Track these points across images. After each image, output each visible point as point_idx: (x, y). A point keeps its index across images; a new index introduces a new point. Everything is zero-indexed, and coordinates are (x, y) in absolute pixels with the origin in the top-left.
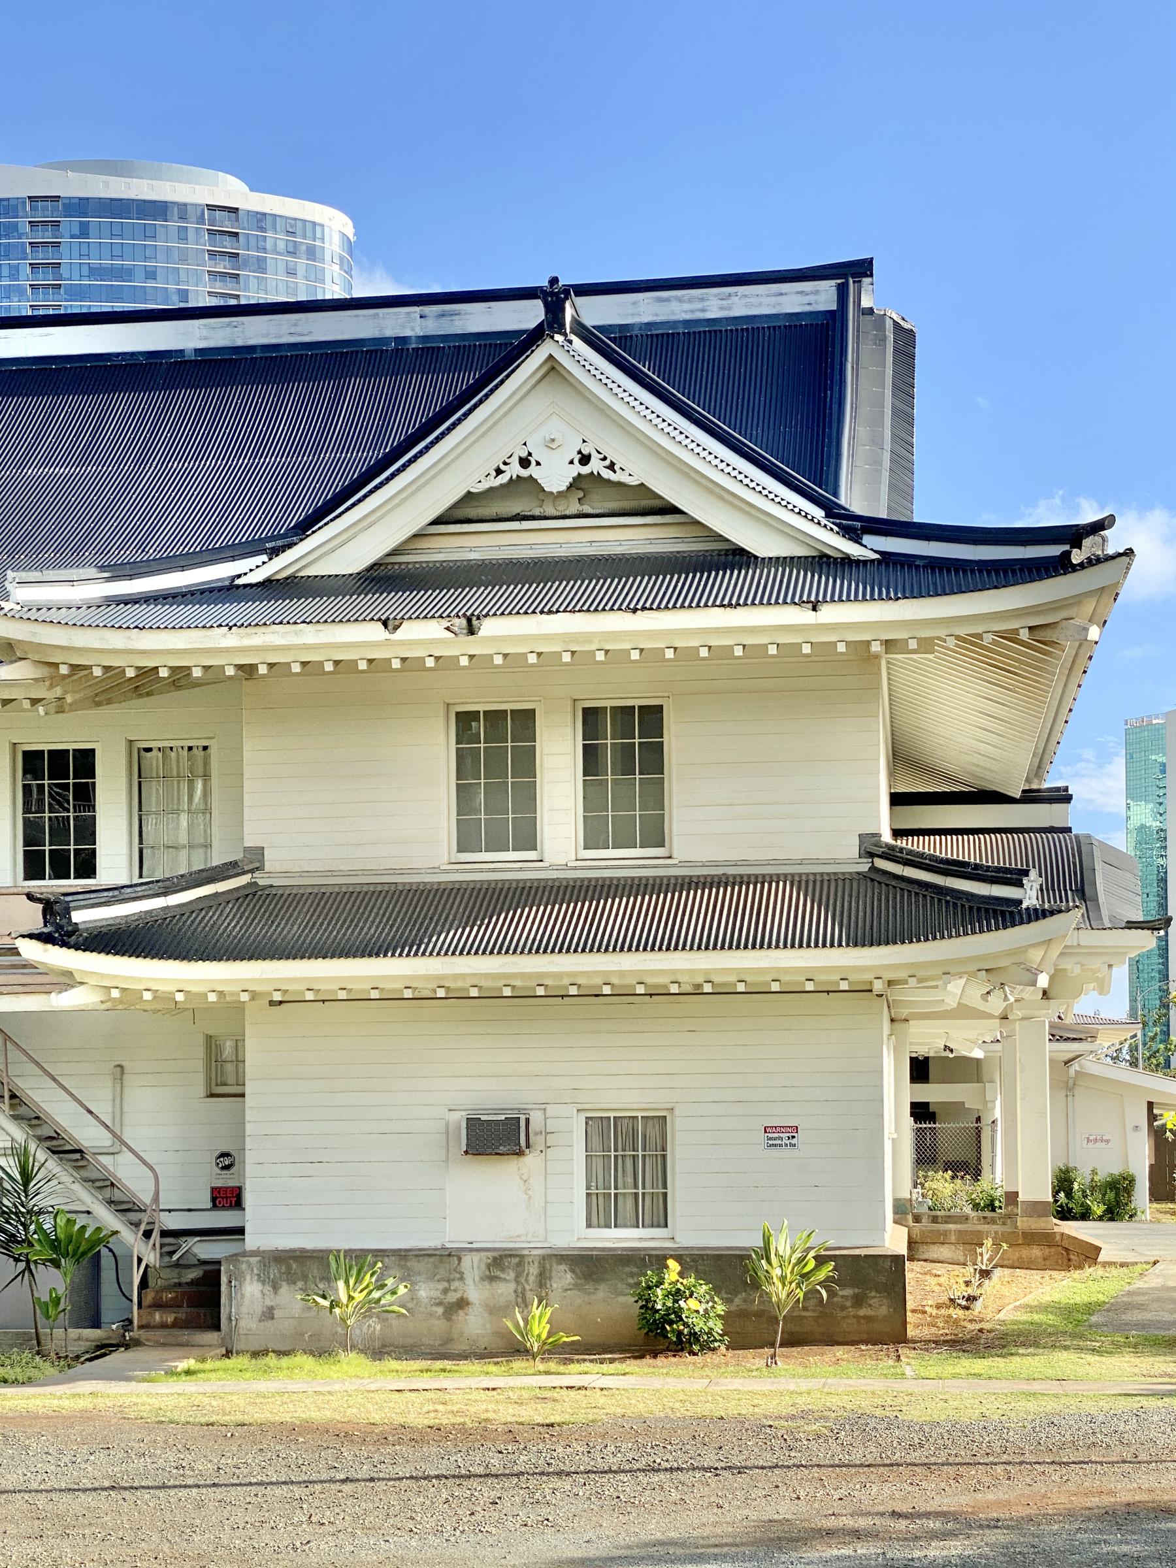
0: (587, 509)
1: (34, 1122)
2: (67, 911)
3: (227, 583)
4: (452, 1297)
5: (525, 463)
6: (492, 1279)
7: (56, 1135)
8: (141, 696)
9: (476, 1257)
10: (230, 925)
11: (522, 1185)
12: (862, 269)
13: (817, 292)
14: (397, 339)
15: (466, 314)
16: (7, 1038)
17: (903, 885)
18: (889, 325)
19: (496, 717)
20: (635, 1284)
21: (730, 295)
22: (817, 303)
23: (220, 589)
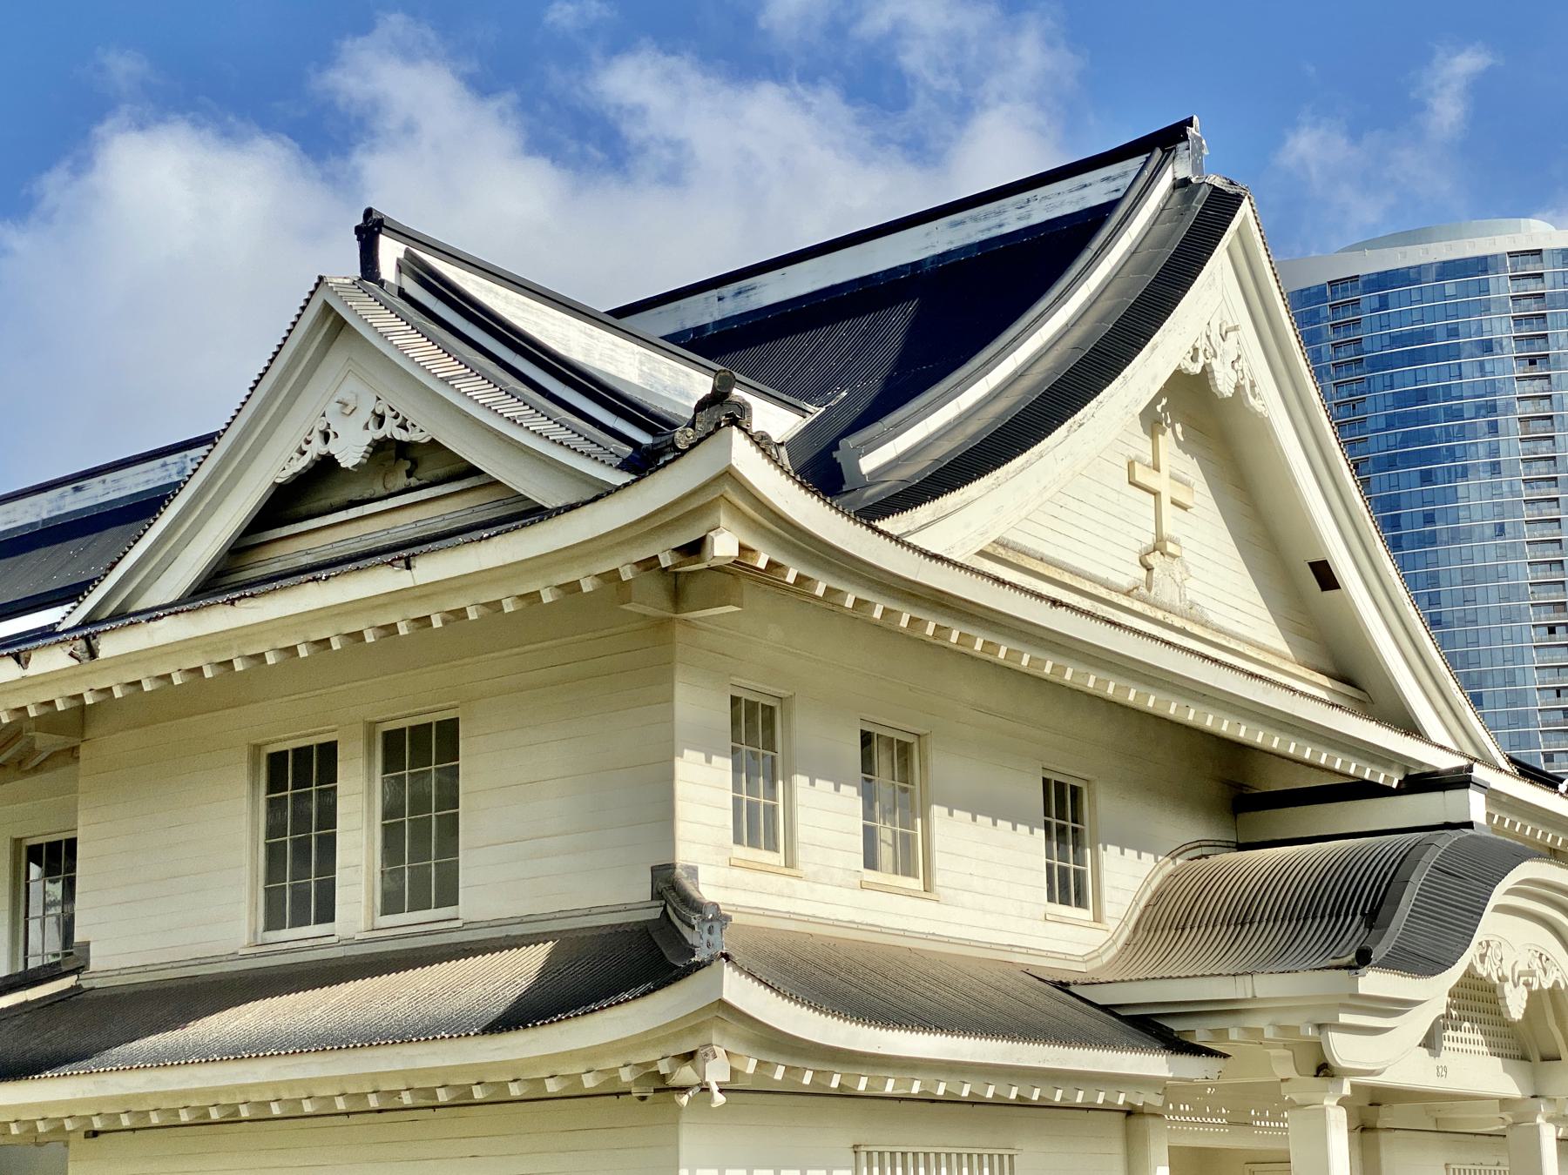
21: (1028, 201)
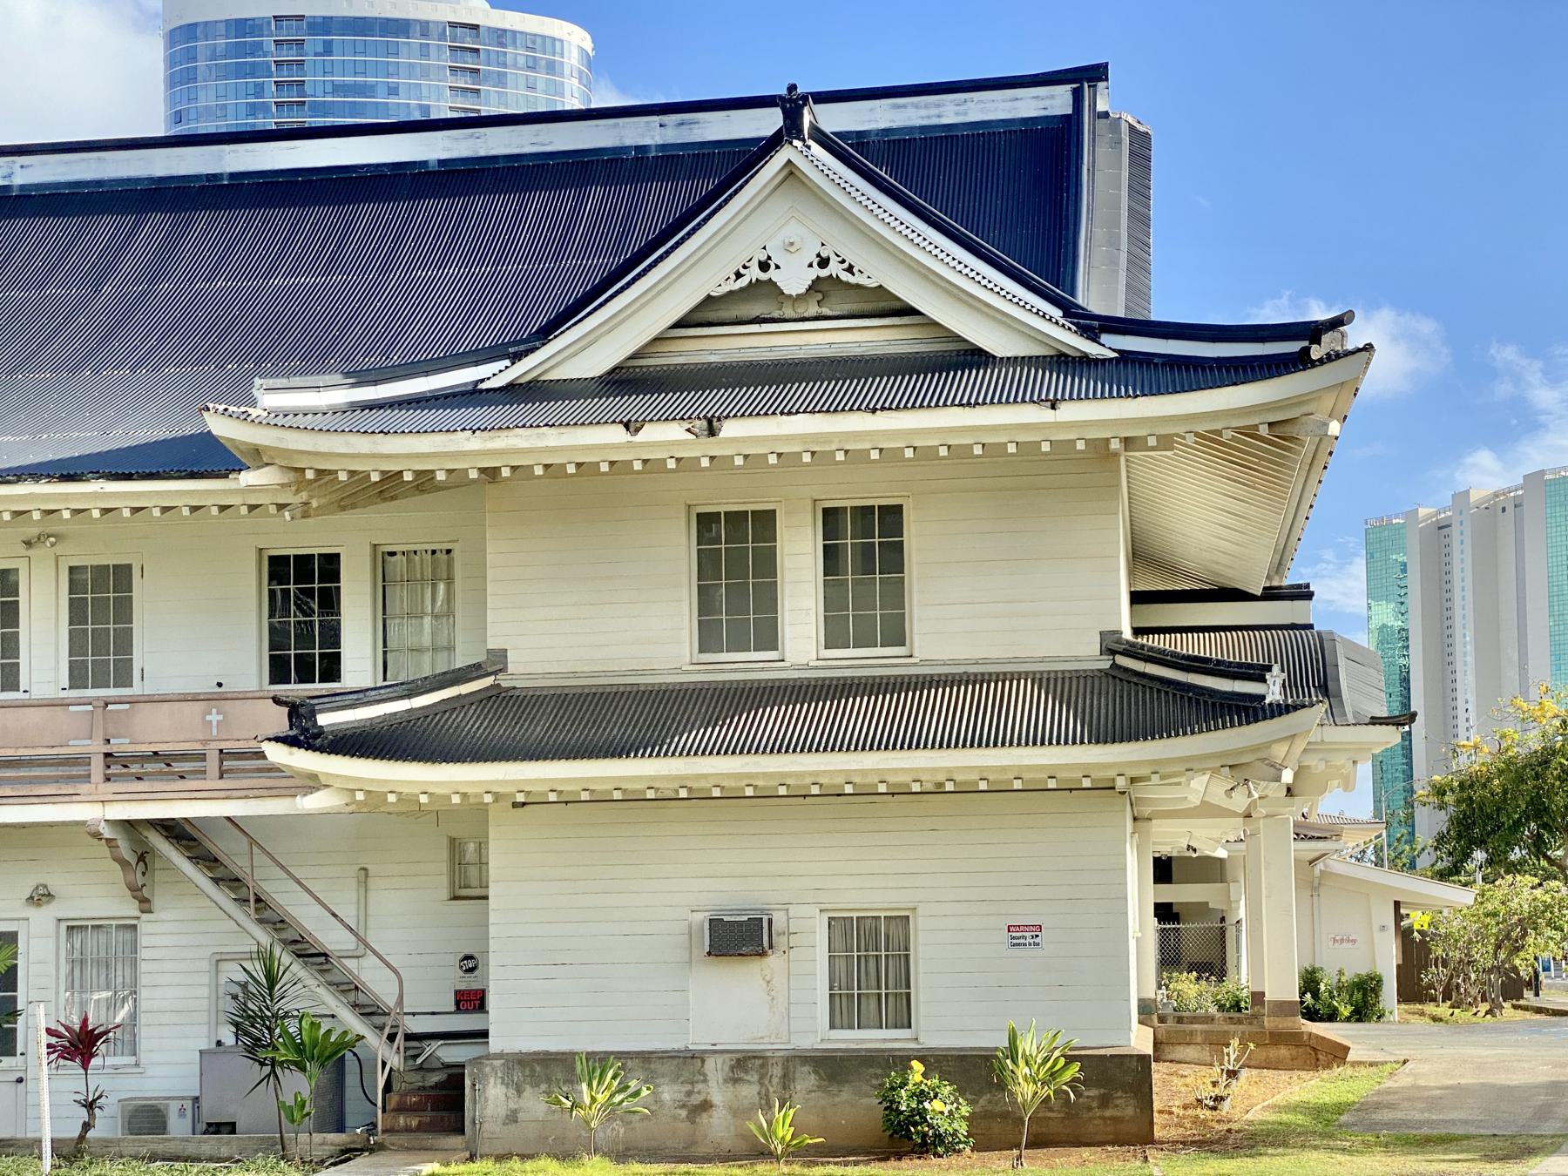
0: (826, 311)
1: (278, 926)
2: (312, 714)
3: (470, 388)
4: (696, 1099)
5: (764, 266)
6: (735, 1081)
7: (300, 939)
8: (385, 500)
9: (720, 1059)
10: (473, 726)
11: (765, 985)
12: (1096, 73)
13: (1052, 97)
14: (637, 148)
15: (704, 122)
16: (253, 842)
17: (1145, 682)
18: (1124, 128)
19: (736, 518)
20: (880, 1085)
21: (965, 101)
22: (1052, 108)
23: (463, 394)
